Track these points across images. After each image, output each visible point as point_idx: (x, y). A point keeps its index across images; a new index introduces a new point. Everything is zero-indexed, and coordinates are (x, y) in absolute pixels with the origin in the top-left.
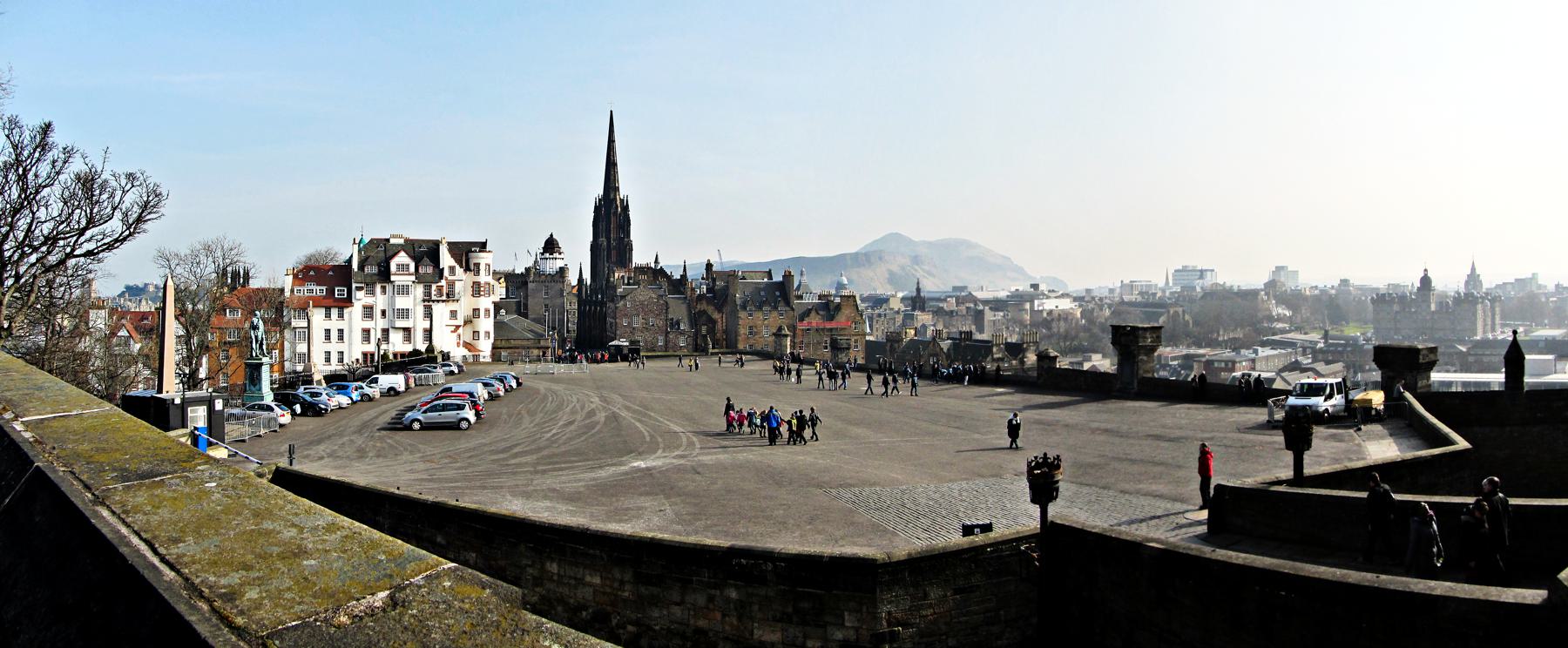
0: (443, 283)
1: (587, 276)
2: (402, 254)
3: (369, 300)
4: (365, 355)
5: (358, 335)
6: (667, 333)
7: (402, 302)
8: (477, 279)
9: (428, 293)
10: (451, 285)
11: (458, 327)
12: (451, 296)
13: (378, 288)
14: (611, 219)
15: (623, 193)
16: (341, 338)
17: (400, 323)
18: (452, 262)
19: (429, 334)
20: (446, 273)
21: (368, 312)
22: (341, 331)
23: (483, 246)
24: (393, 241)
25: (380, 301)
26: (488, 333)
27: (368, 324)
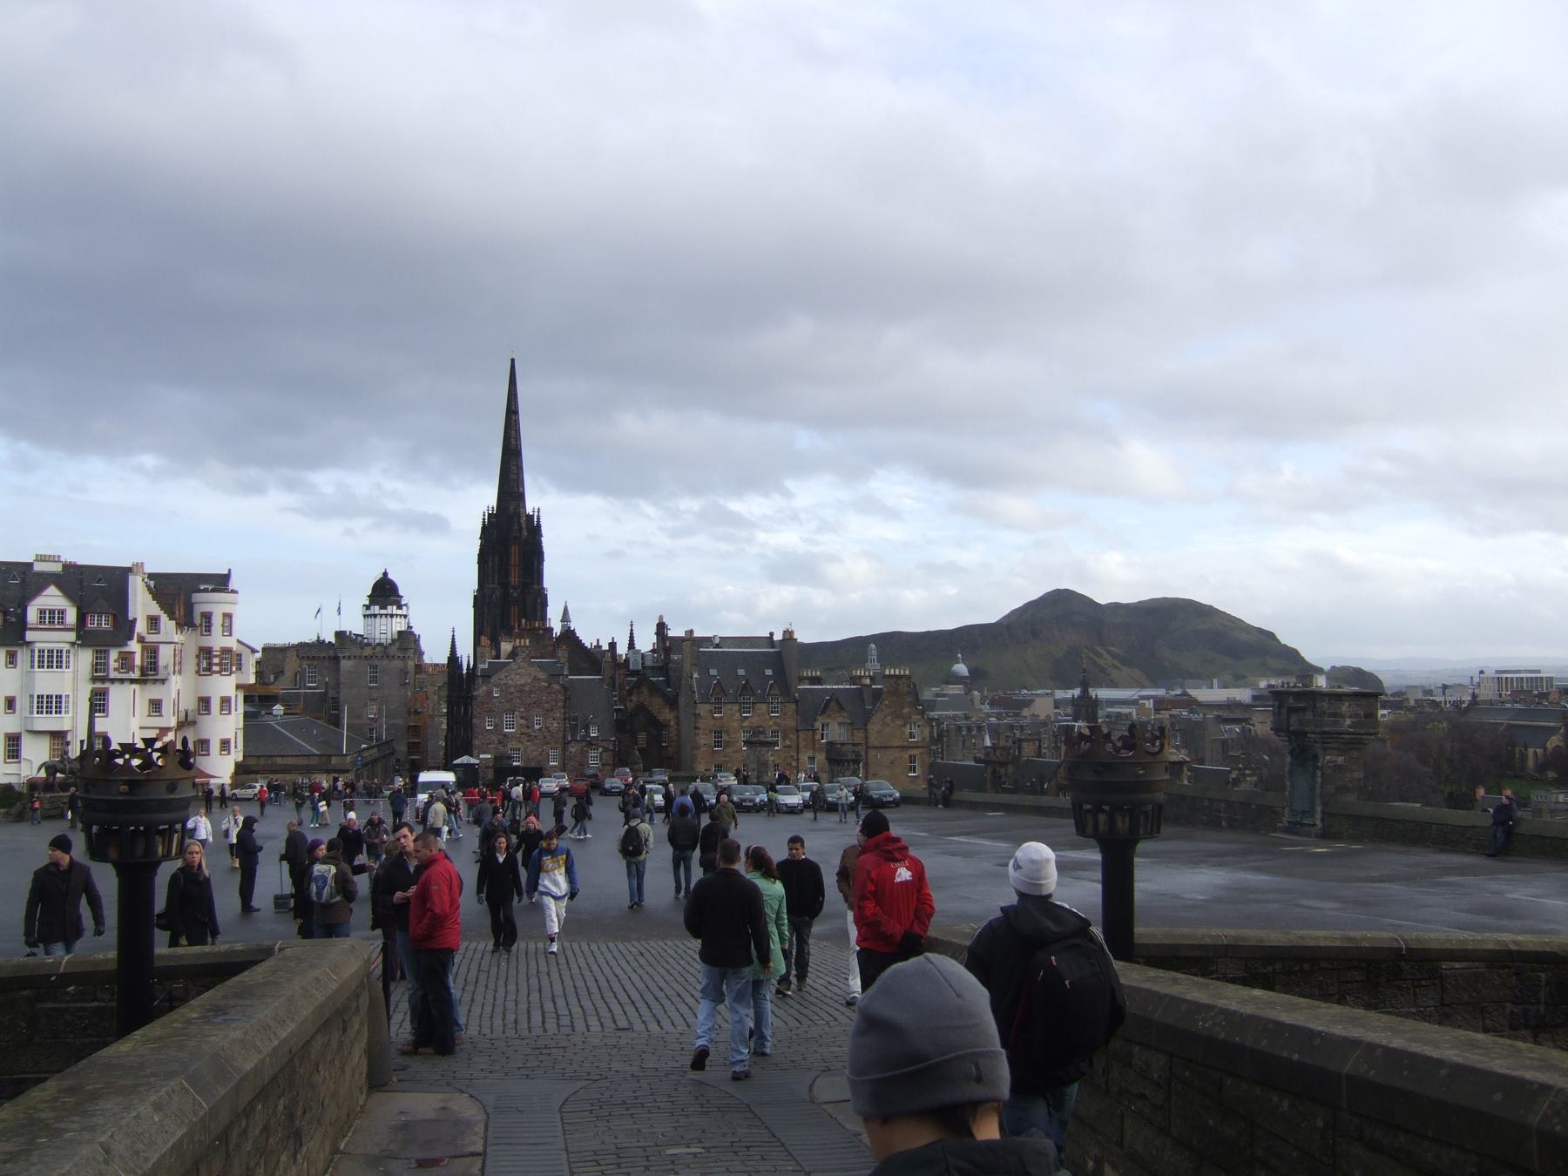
0: (134, 646)
1: (466, 651)
2: (52, 590)
6: (566, 744)
7: (47, 682)
8: (207, 642)
10: (152, 651)
12: (150, 673)
14: (511, 548)
15: (530, 505)
18: (155, 609)
20: (141, 627)
23: (221, 582)
24: (38, 567)
26: (225, 744)
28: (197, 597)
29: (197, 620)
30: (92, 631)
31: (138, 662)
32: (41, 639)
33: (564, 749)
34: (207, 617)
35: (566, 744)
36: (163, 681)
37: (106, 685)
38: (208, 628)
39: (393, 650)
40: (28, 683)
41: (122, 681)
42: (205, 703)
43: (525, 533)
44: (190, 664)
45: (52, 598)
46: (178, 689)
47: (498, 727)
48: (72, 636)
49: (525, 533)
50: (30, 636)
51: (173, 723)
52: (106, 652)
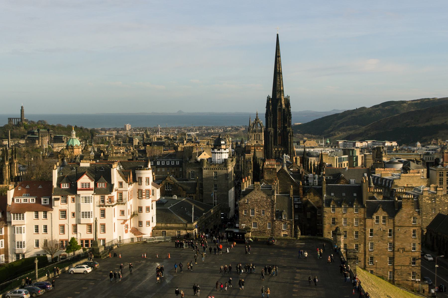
0: (114, 194)
3: (64, 207)
5: (56, 230)
6: (273, 221)
10: (121, 194)
12: (121, 201)
13: (70, 198)
16: (46, 231)
17: (83, 220)
18: (121, 179)
20: (116, 186)
21: (64, 214)
22: (46, 227)
25: (71, 207)
29: (137, 180)
34: (140, 178)
35: (273, 221)
36: (124, 204)
37: (104, 207)
41: (109, 206)
42: (140, 209)
43: (284, 106)
45: (85, 179)
46: (131, 205)
48: (93, 192)
50: (78, 192)
51: (129, 217)
52: (104, 197)
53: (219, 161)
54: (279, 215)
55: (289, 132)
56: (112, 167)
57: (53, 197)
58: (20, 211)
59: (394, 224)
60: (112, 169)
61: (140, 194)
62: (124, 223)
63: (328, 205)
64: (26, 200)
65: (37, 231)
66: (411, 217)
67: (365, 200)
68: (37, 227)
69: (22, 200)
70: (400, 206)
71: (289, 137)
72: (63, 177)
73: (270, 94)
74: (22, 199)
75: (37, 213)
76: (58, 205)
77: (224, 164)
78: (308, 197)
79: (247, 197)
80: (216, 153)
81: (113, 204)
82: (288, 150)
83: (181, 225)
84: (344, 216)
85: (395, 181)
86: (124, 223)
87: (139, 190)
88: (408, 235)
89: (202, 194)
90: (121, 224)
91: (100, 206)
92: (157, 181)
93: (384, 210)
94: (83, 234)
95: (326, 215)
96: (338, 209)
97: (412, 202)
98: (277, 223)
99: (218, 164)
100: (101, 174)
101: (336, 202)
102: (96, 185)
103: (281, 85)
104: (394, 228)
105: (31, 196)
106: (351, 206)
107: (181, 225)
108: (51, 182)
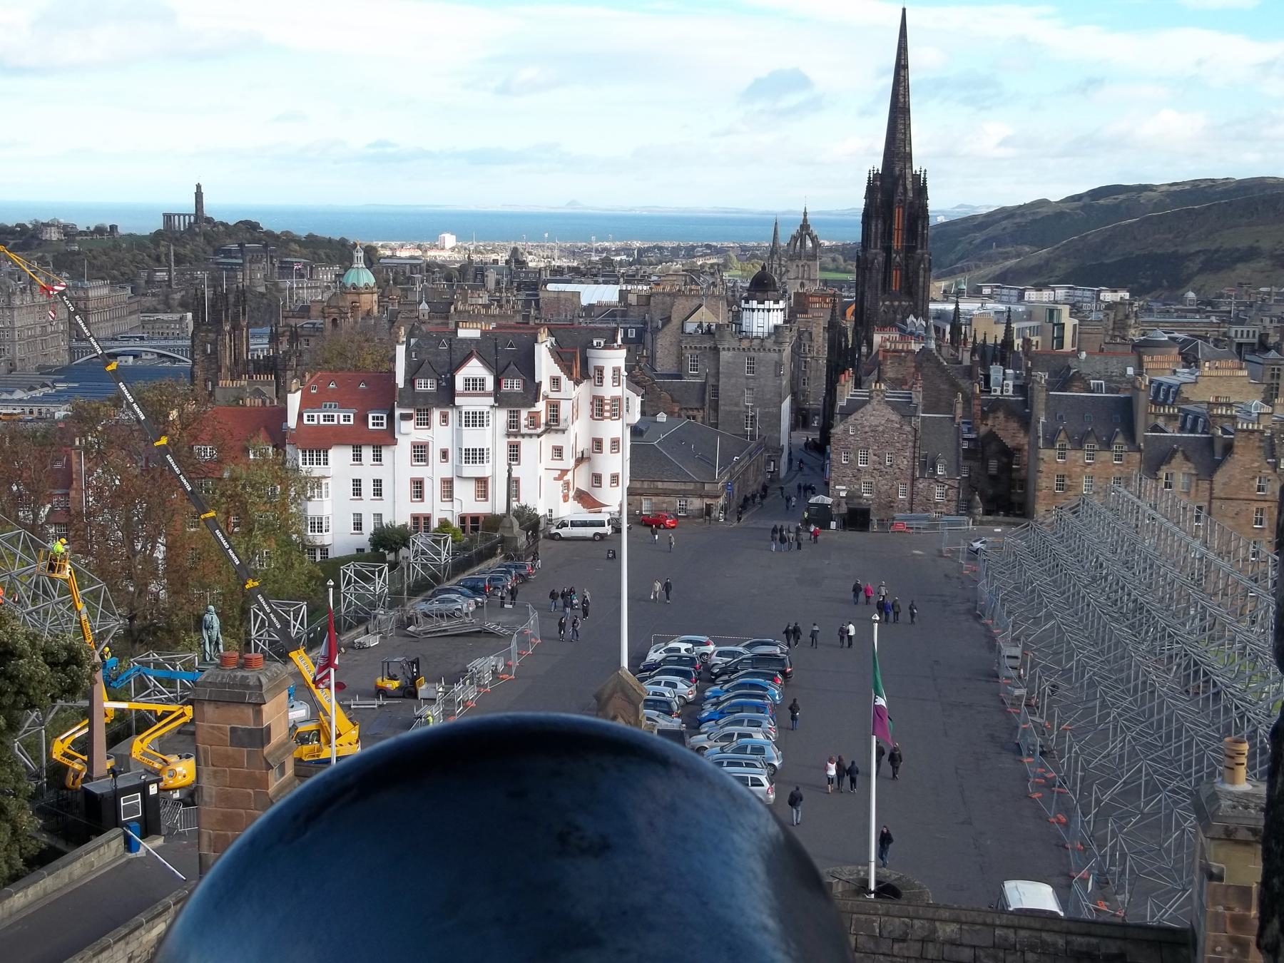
0: (541, 406)
3: (421, 435)
4: (416, 518)
5: (406, 489)
6: (914, 479)
7: (473, 438)
9: (513, 424)
10: (554, 407)
11: (564, 472)
12: (554, 423)
13: (436, 415)
16: (378, 492)
18: (557, 371)
19: (513, 485)
20: (546, 388)
21: (420, 452)
22: (378, 483)
25: (439, 434)
27: (420, 471)
28: (591, 353)
29: (592, 373)
30: (507, 394)
31: (543, 420)
32: (467, 404)
33: (912, 485)
34: (600, 370)
35: (914, 479)
36: (564, 431)
37: (519, 439)
38: (601, 380)
39: (769, 343)
40: (459, 437)
41: (531, 436)
42: (598, 444)
43: (911, 194)
44: (585, 409)
45: (474, 369)
46: (578, 432)
47: (852, 463)
48: (491, 400)
49: (911, 194)
50: (458, 401)
51: (572, 462)
52: (518, 412)
53: (761, 330)
54: (927, 465)
55: (921, 260)
56: (536, 341)
57: (398, 412)
58: (318, 443)
59: (1211, 494)
60: (537, 346)
61: (599, 408)
62: (560, 478)
63: (1050, 443)
64: (326, 418)
65: (357, 491)
66: (1254, 478)
67: (1142, 433)
68: (357, 483)
69: (319, 418)
70: (1228, 448)
71: (921, 272)
72: (420, 365)
73: (878, 164)
74: (321, 415)
75: (357, 449)
76: (408, 432)
77: (773, 338)
78: (990, 423)
79: (851, 419)
80: (753, 310)
81: (539, 431)
82: (916, 304)
83: (691, 486)
84: (1088, 470)
85: (1183, 388)
86: (560, 478)
87: (594, 397)
88: (1243, 521)
89: (716, 410)
90: (555, 479)
91: (508, 435)
92: (637, 376)
93: (1187, 458)
94: (467, 502)
95: (1042, 467)
96: (1073, 452)
97: (1261, 441)
98: (921, 485)
99: (757, 337)
100: (512, 362)
101: (1069, 438)
102: (498, 383)
103: (907, 140)
104: (1210, 503)
105: (343, 407)
106: (1107, 446)
107: (691, 486)
108: (392, 374)
